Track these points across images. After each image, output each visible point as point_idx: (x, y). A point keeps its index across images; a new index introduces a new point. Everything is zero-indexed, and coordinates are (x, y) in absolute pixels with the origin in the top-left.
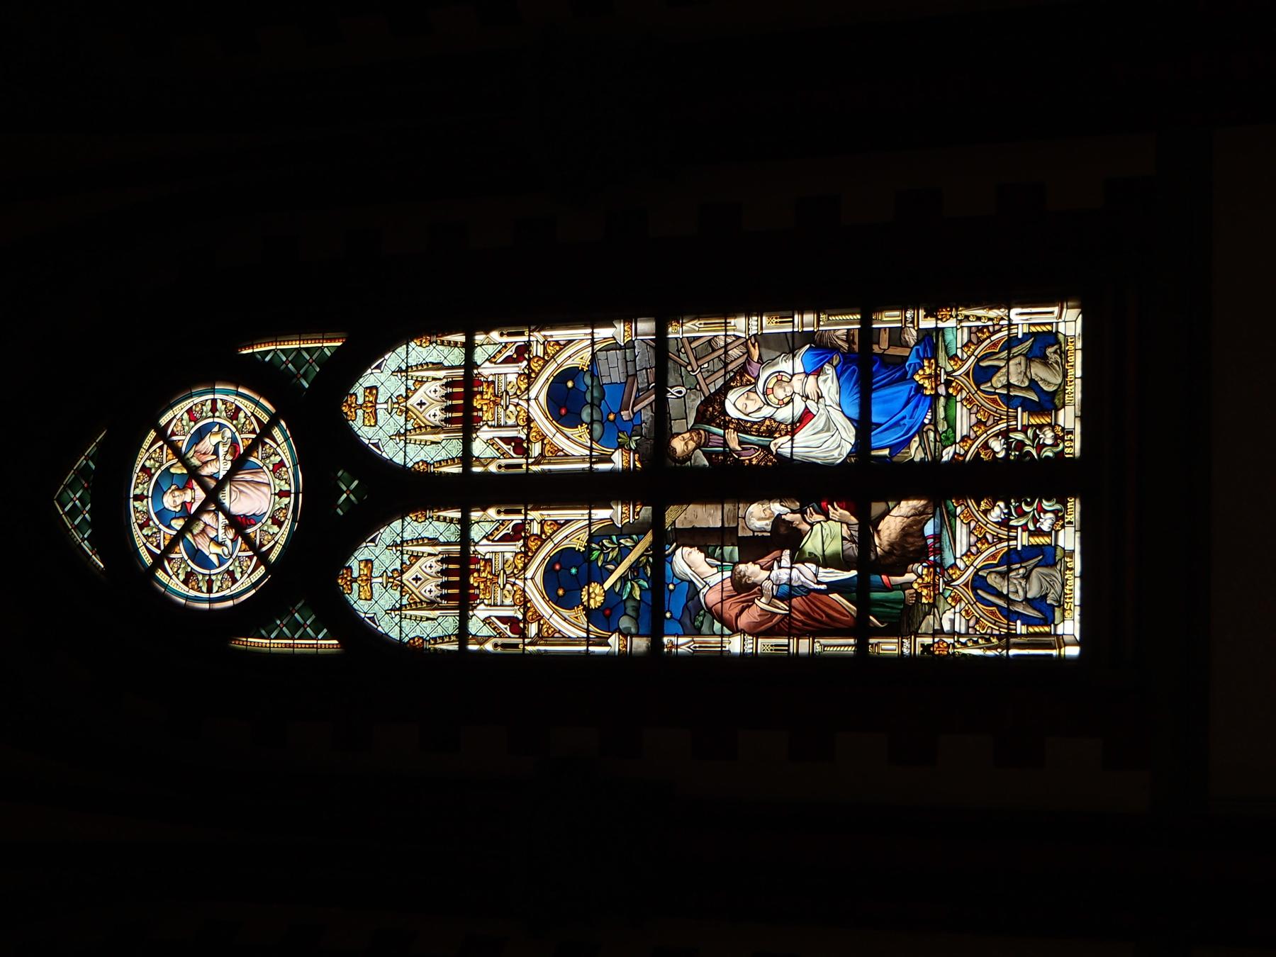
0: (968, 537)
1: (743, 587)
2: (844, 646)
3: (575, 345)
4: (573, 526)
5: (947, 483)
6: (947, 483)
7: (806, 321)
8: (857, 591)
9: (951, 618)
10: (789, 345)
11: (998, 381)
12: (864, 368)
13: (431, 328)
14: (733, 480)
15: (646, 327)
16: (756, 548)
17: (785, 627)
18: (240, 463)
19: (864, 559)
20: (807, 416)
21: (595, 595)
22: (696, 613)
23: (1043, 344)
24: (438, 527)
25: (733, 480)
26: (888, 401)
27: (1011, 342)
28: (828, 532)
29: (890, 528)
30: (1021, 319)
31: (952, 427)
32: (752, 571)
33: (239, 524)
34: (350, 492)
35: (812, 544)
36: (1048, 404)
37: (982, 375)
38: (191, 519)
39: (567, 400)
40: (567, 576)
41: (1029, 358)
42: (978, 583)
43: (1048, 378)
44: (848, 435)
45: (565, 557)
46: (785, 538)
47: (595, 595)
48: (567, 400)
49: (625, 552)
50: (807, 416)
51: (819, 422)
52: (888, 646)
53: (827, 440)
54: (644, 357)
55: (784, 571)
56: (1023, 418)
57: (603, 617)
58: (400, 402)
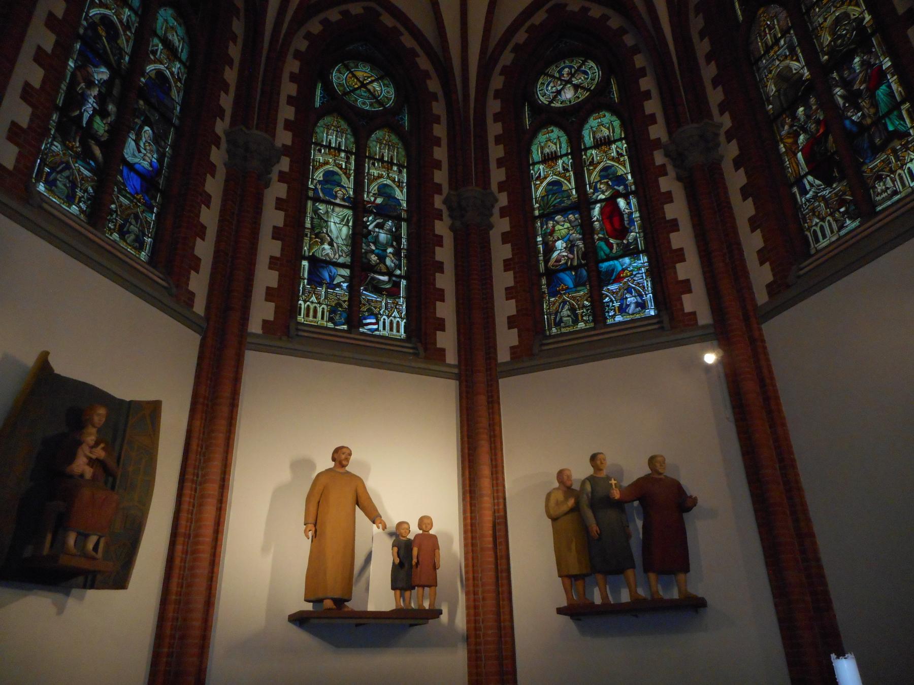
2: (60, 101)
9: (57, 147)
10: (160, 160)
11: (133, 222)
12: (149, 180)
13: (623, 125)
19: (88, 133)
20: (139, 151)
26: (136, 182)
27: (144, 235)
29: (97, 152)
31: (125, 197)
32: (95, 92)
35: (98, 119)
37: (137, 217)
41: (137, 236)
42: (68, 167)
44: (130, 159)
46: (101, 112)
49: (114, 55)
50: (139, 151)
51: (136, 153)
56: (120, 221)
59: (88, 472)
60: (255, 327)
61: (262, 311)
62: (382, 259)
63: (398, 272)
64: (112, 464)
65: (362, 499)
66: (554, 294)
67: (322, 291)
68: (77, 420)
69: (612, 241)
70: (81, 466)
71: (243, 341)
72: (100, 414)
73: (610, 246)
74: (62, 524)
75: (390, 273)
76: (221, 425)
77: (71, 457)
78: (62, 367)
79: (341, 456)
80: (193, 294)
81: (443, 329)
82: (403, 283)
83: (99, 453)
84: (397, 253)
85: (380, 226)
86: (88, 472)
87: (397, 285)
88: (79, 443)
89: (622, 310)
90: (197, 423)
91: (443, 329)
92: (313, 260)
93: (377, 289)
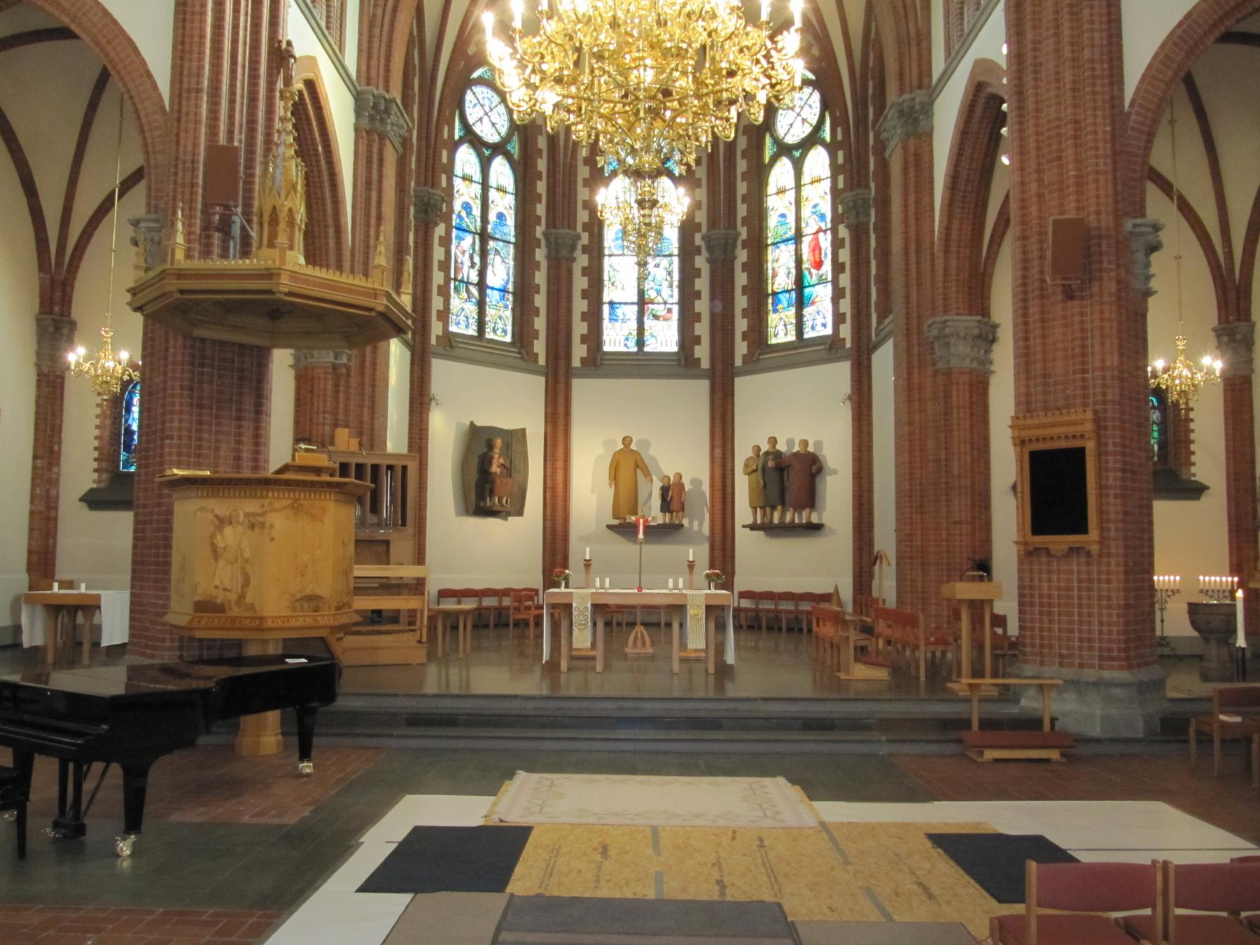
0: (471, 309)
1: (464, 252)
3: (511, 221)
4: (477, 212)
5: (481, 305)
6: (481, 305)
7: (512, 279)
8: (462, 281)
12: (503, 290)
14: (484, 254)
15: (513, 240)
16: (471, 257)
17: (456, 262)
18: (493, 124)
21: (464, 214)
22: (460, 239)
23: (504, 331)
24: (477, 177)
25: (484, 254)
28: (474, 277)
30: (509, 329)
32: (467, 255)
33: (481, 119)
34: (486, 152)
36: (494, 331)
37: (500, 317)
38: (482, 106)
39: (501, 216)
40: (467, 207)
43: (499, 332)
45: (471, 208)
46: (473, 265)
47: (464, 214)
48: (501, 216)
52: (452, 286)
53: (491, 280)
54: (508, 238)
55: (467, 263)
57: (459, 216)
58: (502, 172)
59: (498, 470)
60: (576, 363)
61: (579, 351)
62: (659, 293)
63: (670, 301)
64: (507, 465)
65: (640, 464)
66: (775, 311)
67: (618, 325)
68: (490, 446)
69: (813, 271)
70: (495, 468)
71: (570, 373)
72: (498, 442)
73: (810, 274)
74: (492, 493)
75: (665, 303)
76: (561, 428)
77: (490, 464)
78: (478, 424)
79: (627, 441)
80: (537, 355)
81: (699, 343)
82: (676, 309)
83: (501, 461)
84: (671, 286)
85: (657, 266)
86: (498, 470)
87: (670, 311)
88: (492, 458)
89: (813, 328)
90: (549, 429)
91: (699, 343)
92: (611, 303)
93: (656, 317)
